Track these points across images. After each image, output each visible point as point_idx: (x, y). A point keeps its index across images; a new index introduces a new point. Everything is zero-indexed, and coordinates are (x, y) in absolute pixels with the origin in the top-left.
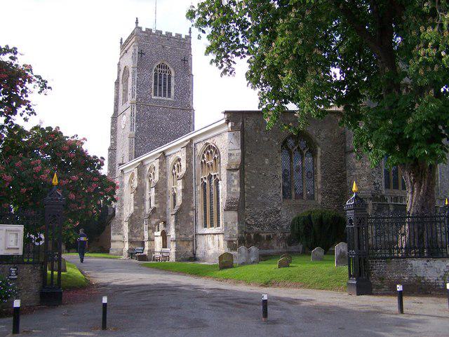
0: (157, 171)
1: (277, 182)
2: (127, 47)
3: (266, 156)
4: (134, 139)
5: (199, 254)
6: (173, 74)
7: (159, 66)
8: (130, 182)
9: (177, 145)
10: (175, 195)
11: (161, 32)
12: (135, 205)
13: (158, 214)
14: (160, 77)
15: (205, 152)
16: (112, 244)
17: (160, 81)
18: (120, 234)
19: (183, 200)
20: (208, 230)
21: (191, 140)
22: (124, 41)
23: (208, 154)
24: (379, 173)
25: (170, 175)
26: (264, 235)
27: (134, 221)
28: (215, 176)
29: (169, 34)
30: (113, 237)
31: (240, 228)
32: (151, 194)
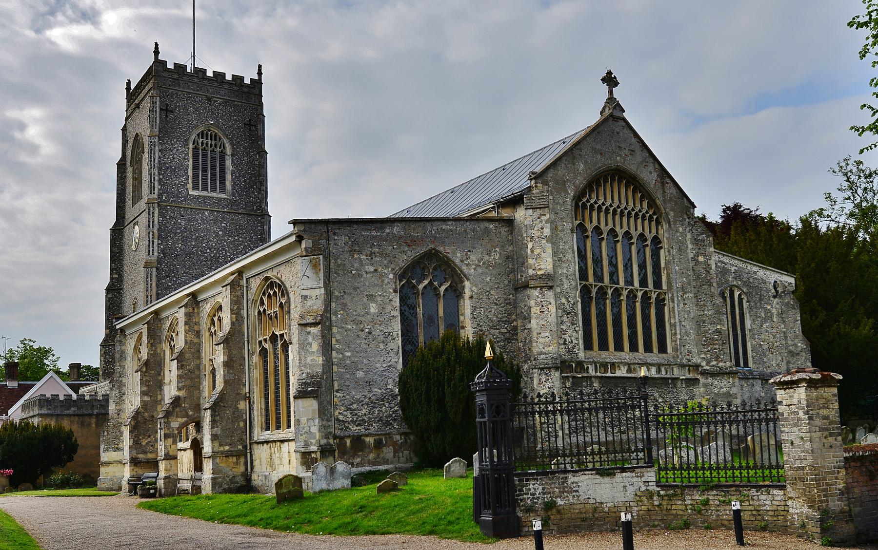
0: (181, 328)
1: (391, 345)
3: (371, 297)
4: (154, 270)
5: (257, 479)
6: (229, 150)
7: (201, 135)
8: (137, 350)
9: (216, 282)
10: (213, 372)
11: (204, 71)
12: (143, 394)
13: (186, 408)
14: (205, 156)
15: (264, 294)
16: (103, 470)
17: (205, 163)
19: (226, 382)
20: (267, 435)
21: (240, 272)
22: (133, 87)
23: (269, 296)
24: (573, 324)
25: (205, 335)
26: (370, 440)
27: (141, 425)
28: (282, 336)
29: (219, 76)
30: (105, 457)
31: (323, 428)
32: (171, 372)
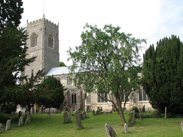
2: (37, 24)
6: (54, 39)
18: (90, 103)
